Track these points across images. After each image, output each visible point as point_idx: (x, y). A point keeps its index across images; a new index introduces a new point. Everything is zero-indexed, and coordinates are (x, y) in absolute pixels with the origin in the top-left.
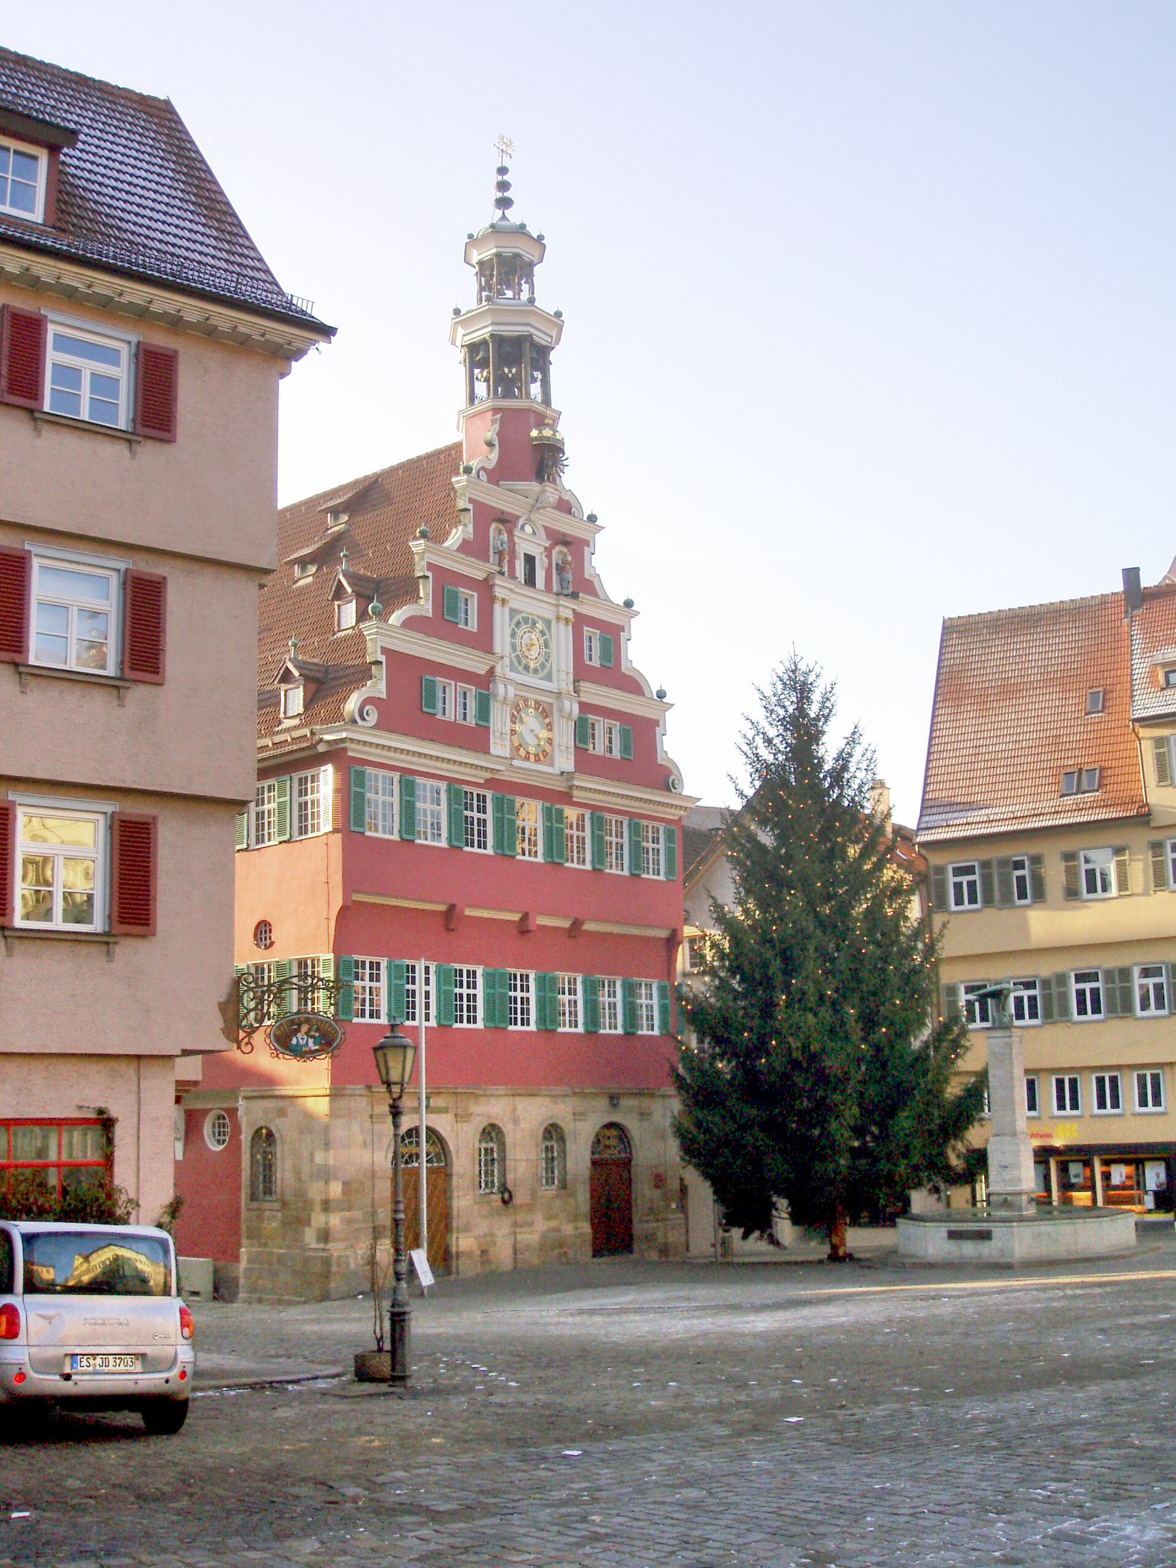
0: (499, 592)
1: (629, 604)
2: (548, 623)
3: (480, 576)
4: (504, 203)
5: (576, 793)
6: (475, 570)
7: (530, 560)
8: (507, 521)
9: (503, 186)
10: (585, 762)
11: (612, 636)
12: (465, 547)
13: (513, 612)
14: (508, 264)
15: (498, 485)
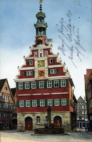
0: (35, 59)
1: (58, 54)
2: (44, 60)
3: (33, 58)
4: (41, 10)
5: (49, 79)
6: (32, 58)
7: (41, 54)
8: (37, 50)
9: (41, 7)
10: (50, 75)
11: (55, 58)
12: (31, 56)
13: (38, 61)
14: (41, 17)
15: (36, 47)
